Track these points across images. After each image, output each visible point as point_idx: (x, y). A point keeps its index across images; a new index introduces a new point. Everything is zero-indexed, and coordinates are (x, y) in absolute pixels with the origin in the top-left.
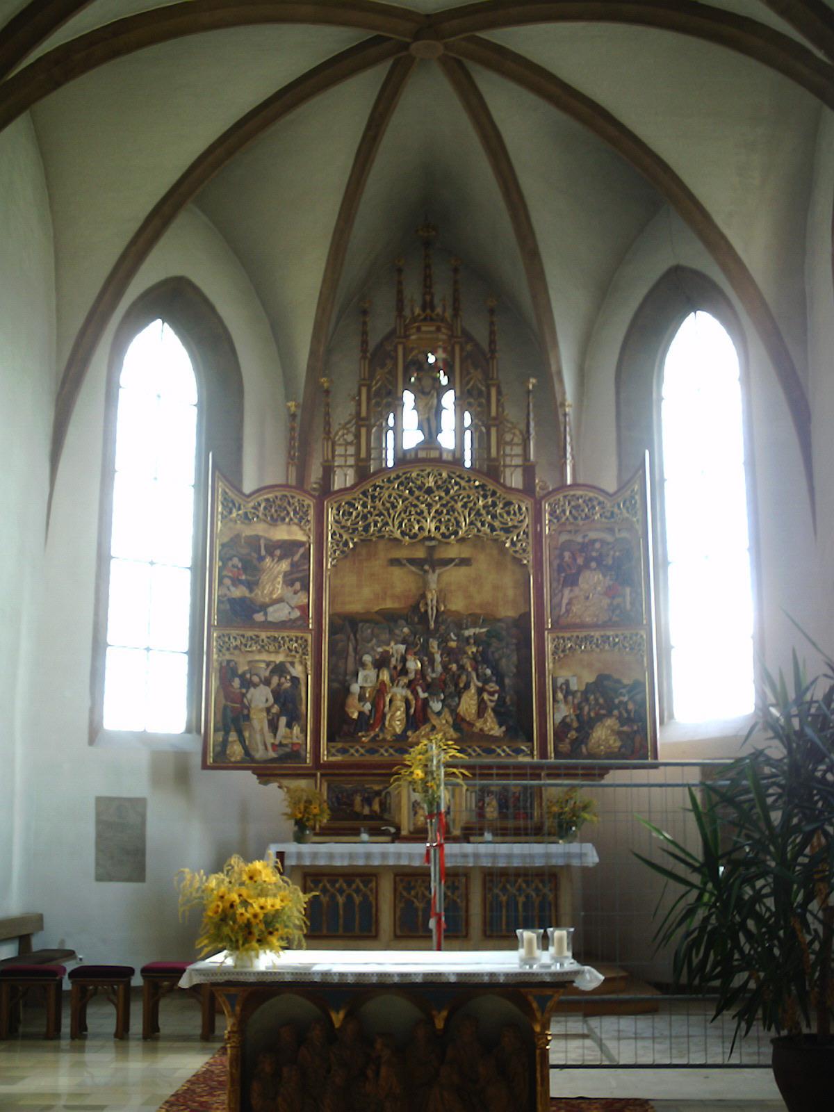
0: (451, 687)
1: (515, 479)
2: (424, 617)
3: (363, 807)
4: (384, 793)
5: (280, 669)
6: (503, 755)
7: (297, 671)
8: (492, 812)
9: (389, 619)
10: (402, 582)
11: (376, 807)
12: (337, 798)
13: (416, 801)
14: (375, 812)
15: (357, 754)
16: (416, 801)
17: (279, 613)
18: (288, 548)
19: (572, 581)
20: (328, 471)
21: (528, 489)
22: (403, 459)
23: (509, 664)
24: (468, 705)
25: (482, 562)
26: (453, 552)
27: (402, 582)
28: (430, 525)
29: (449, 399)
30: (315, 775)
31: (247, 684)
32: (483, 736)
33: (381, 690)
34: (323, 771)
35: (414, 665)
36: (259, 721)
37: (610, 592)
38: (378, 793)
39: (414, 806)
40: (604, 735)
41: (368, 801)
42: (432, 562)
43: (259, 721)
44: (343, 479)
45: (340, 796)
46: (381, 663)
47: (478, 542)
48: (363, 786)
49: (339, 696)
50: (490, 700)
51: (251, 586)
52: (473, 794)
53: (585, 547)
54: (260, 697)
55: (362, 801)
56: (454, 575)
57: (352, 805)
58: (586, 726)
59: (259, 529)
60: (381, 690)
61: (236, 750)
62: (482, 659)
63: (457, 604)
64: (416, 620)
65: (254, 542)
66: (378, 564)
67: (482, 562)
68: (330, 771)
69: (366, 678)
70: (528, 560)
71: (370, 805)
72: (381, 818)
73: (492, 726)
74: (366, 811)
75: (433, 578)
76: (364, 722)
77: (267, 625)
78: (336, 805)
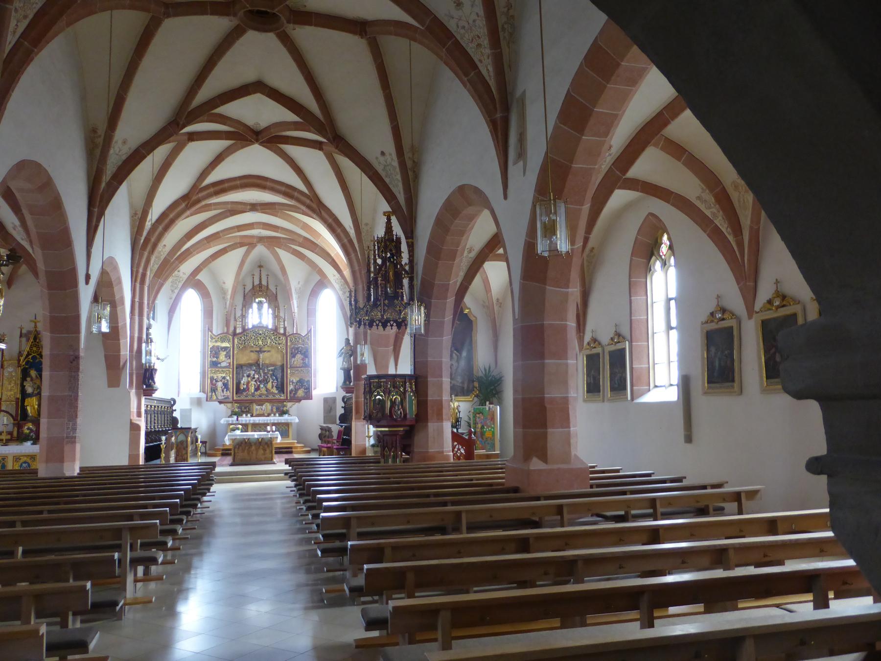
0: (265, 381)
1: (282, 331)
2: (259, 365)
5: (224, 378)
6: (277, 397)
7: (228, 378)
8: (275, 410)
9: (250, 365)
10: (254, 356)
15: (243, 397)
17: (223, 364)
18: (225, 349)
19: (294, 357)
20: (235, 329)
21: (284, 334)
22: (254, 327)
23: (279, 376)
24: (269, 385)
25: (273, 352)
26: (266, 349)
27: (254, 356)
28: (260, 343)
29: (266, 305)
31: (217, 381)
32: (273, 393)
33: (248, 383)
35: (256, 376)
36: (219, 389)
37: (303, 359)
40: (301, 393)
42: (260, 351)
43: (219, 389)
44: (239, 331)
46: (248, 376)
47: (272, 347)
49: (238, 384)
50: (275, 385)
51: (217, 358)
53: (297, 349)
54: (220, 384)
56: (266, 354)
58: (296, 390)
59: (219, 344)
60: (248, 383)
61: (214, 398)
62: (273, 375)
63: (267, 362)
64: (257, 364)
65: (218, 347)
66: (248, 351)
67: (273, 352)
68: (236, 402)
69: (244, 380)
70: (284, 351)
73: (275, 391)
75: (261, 355)
76: (244, 390)
77: (221, 367)
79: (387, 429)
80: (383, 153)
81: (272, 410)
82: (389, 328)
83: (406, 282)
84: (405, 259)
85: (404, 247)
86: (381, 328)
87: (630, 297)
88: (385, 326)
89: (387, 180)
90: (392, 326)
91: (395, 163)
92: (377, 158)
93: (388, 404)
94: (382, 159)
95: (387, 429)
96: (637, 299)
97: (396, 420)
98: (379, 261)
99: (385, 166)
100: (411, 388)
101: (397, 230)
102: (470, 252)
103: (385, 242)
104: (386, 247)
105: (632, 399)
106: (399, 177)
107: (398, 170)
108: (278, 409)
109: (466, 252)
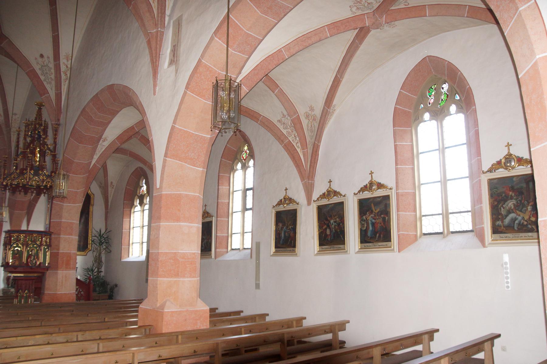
79: (22, 275)
80: (42, 56)
82: (29, 194)
83: (48, 159)
84: (50, 141)
85: (50, 133)
86: (22, 193)
87: (218, 186)
88: (26, 193)
89: (42, 78)
90: (32, 192)
91: (52, 65)
92: (36, 59)
93: (25, 255)
94: (40, 60)
95: (22, 275)
96: (223, 189)
97: (31, 268)
98: (29, 140)
99: (42, 66)
100: (46, 242)
101: (45, 116)
102: (104, 141)
103: (35, 126)
104: (35, 129)
105: (215, 258)
106: (53, 76)
107: (53, 71)
109: (101, 141)
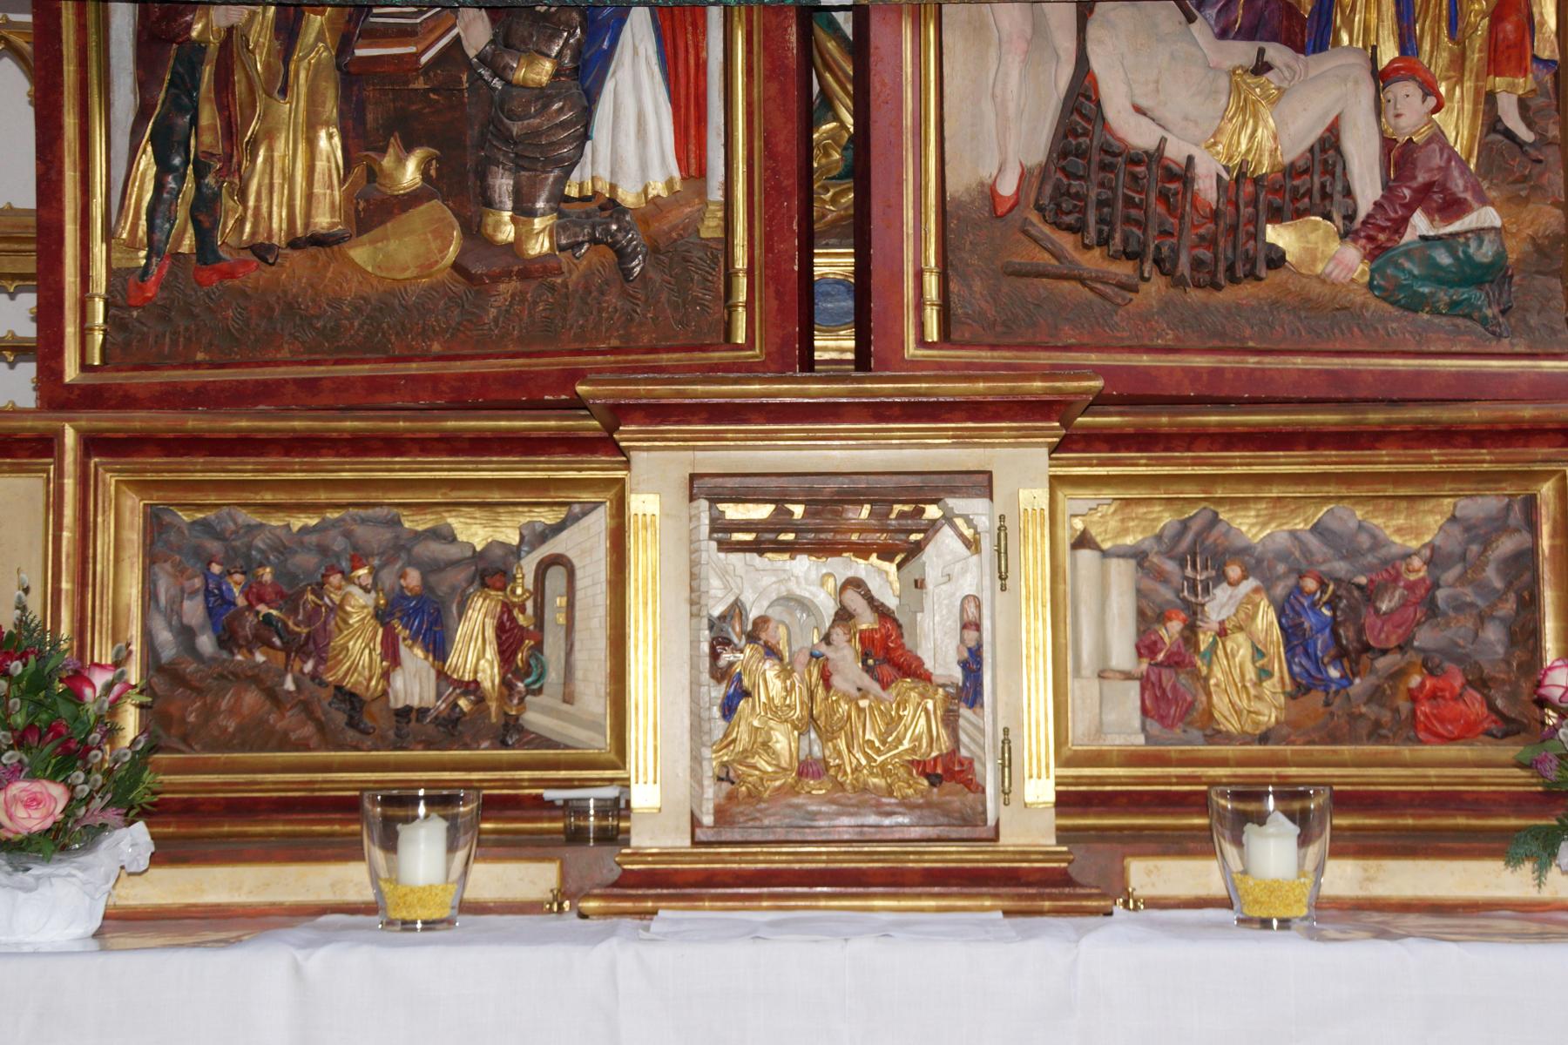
3: (391, 654)
4: (528, 567)
11: (474, 651)
12: (218, 603)
13: (736, 610)
14: (472, 688)
16: (736, 610)
30: (47, 445)
34: (105, 421)
38: (491, 570)
39: (720, 642)
41: (423, 619)
45: (236, 587)
48: (396, 522)
52: (1122, 575)
55: (382, 616)
57: (313, 642)
71: (438, 647)
72: (510, 731)
74: (414, 682)
78: (206, 643)
81: (1169, 676)
108: (1334, 632)
